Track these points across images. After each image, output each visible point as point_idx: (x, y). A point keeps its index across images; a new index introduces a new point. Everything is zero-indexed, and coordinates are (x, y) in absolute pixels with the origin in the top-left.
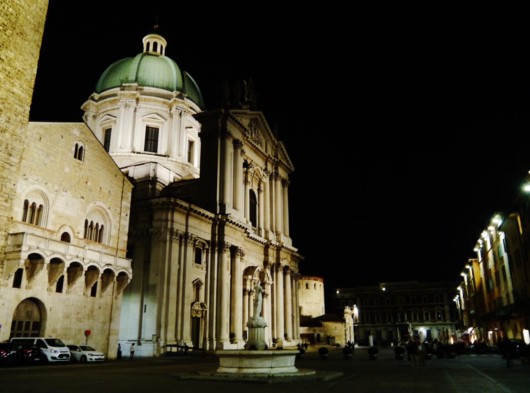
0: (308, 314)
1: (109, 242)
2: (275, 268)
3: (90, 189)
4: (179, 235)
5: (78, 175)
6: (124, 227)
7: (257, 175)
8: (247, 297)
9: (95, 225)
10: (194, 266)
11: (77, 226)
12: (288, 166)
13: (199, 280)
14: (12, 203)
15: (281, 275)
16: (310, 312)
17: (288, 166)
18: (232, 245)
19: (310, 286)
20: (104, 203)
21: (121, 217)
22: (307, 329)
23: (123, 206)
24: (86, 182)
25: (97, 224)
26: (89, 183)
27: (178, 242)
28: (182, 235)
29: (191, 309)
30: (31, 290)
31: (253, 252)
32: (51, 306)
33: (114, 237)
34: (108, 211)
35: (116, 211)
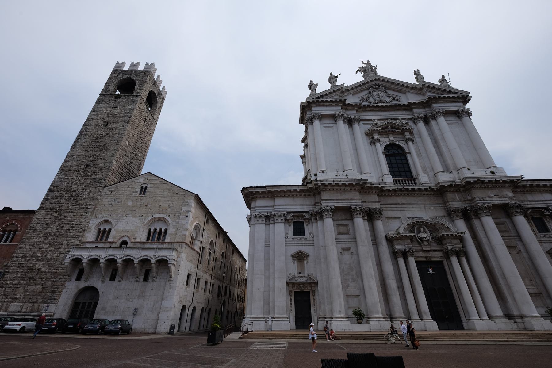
3: (150, 209)
4: (263, 217)
5: (139, 203)
7: (392, 128)
8: (401, 261)
10: (291, 240)
11: (135, 234)
12: (456, 95)
13: (300, 252)
14: (84, 232)
17: (456, 95)
18: (335, 207)
20: (163, 214)
24: (147, 206)
26: (149, 205)
27: (264, 222)
29: (287, 284)
30: (88, 282)
31: (412, 204)
34: (168, 218)
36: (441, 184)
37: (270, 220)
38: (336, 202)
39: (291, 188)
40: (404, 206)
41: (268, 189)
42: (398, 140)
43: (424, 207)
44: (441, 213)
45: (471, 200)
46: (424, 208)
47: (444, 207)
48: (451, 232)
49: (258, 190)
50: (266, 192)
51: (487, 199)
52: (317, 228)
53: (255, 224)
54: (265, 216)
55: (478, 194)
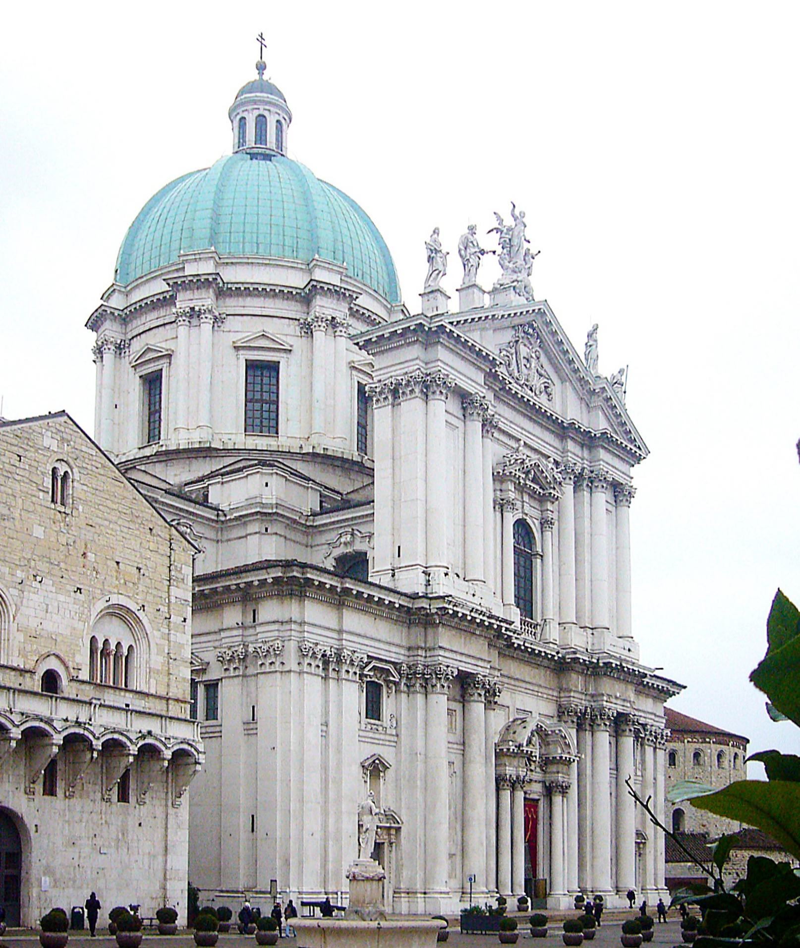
0: (698, 830)
1: (148, 682)
2: (588, 722)
4: (319, 657)
6: (181, 646)
9: (113, 647)
15: (604, 738)
16: (704, 826)
19: (705, 759)
21: (172, 625)
22: (689, 868)
23: (173, 600)
25: (119, 644)
28: (328, 653)
32: (36, 822)
33: (158, 672)
34: (141, 614)
35: (158, 613)
36: (578, 656)
37: (331, 669)
38: (459, 657)
39: (388, 596)
40: (517, 683)
41: (347, 585)
42: (531, 512)
43: (538, 692)
44: (549, 709)
45: (593, 696)
46: (536, 693)
47: (557, 697)
48: (569, 753)
49: (325, 578)
50: (339, 590)
51: (614, 700)
52: (412, 709)
53: (301, 673)
54: (324, 656)
55: (608, 686)
